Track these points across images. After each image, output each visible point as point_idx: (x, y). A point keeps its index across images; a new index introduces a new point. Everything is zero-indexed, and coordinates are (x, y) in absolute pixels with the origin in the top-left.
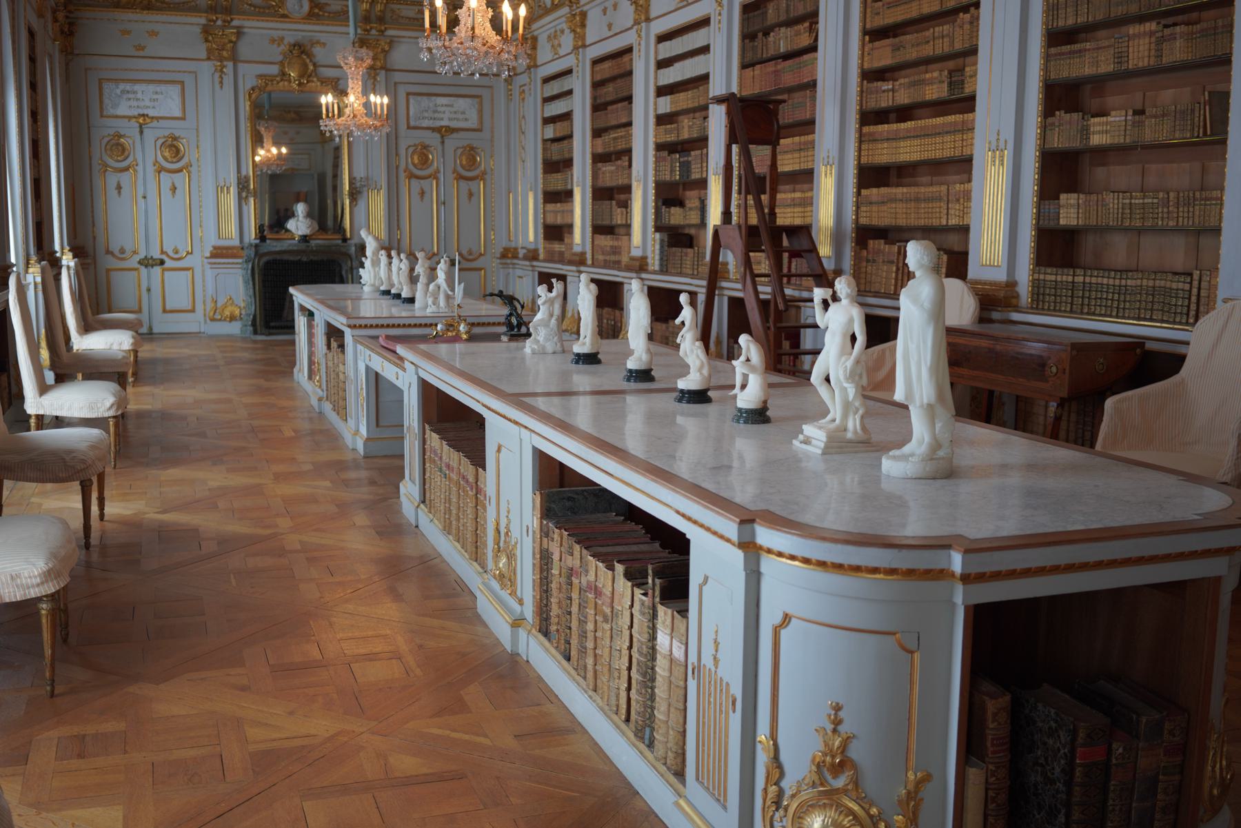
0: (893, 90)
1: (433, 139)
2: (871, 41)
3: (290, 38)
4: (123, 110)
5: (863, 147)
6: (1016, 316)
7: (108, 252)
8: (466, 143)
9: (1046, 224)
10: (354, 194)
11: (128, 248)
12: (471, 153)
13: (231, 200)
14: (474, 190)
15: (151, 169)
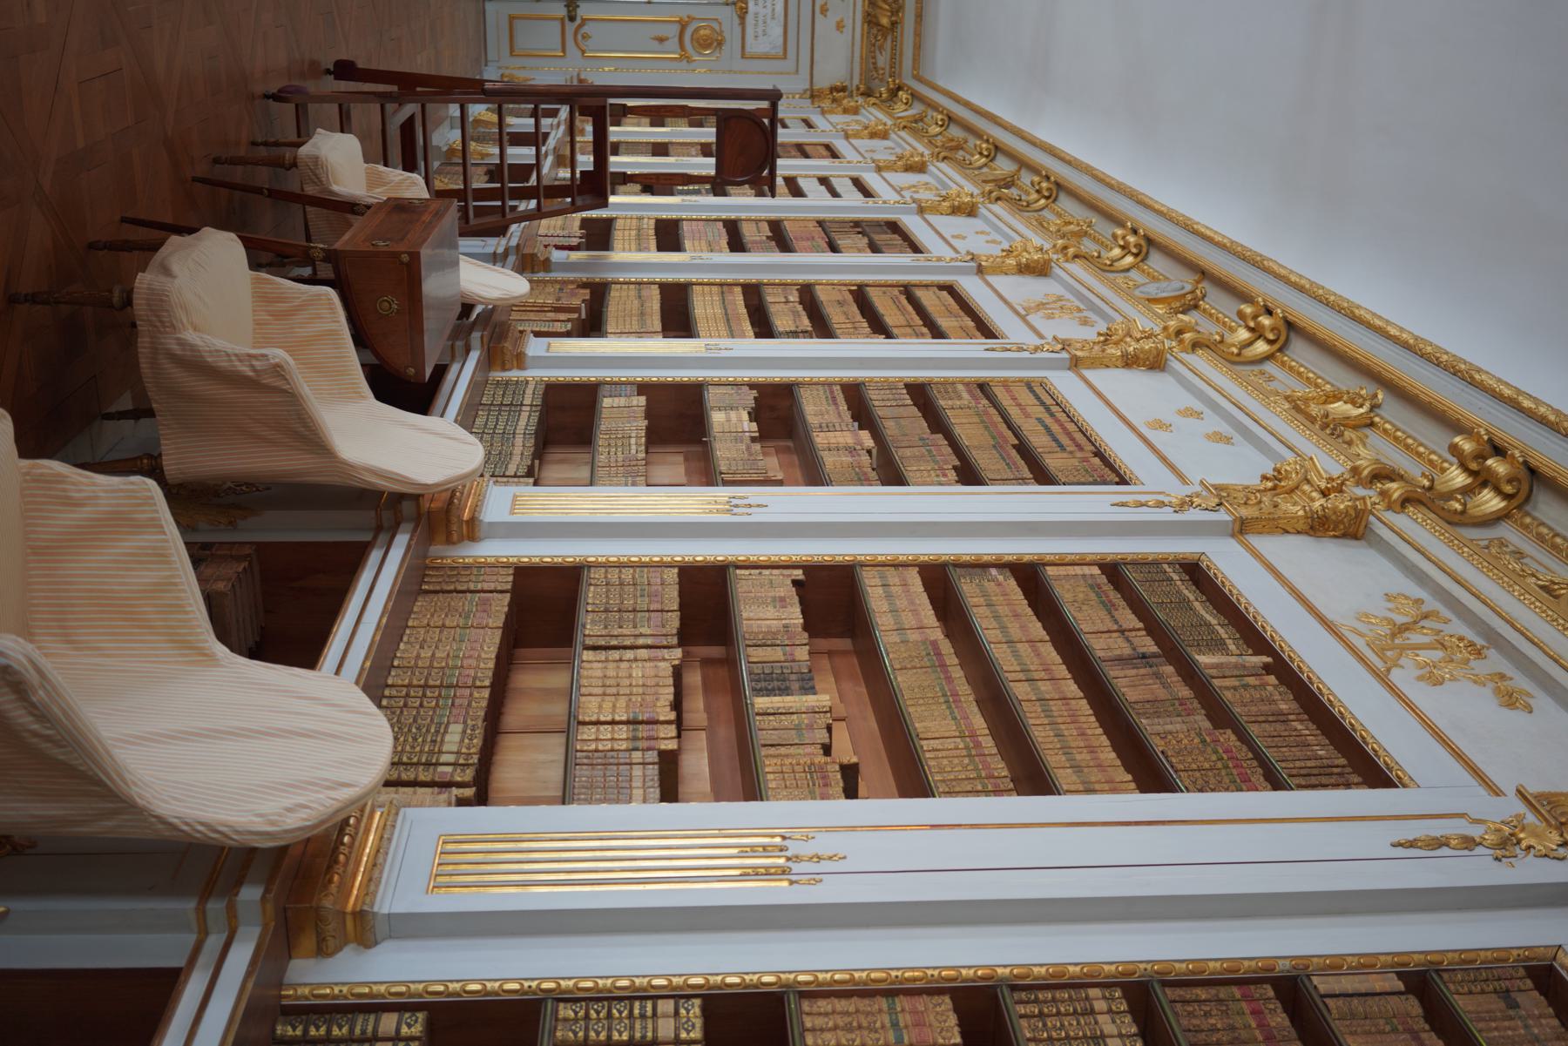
0: (787, 302)
2: (851, 292)
5: (715, 289)
6: (474, 356)
8: (727, 35)
9: (605, 390)
12: (713, 42)
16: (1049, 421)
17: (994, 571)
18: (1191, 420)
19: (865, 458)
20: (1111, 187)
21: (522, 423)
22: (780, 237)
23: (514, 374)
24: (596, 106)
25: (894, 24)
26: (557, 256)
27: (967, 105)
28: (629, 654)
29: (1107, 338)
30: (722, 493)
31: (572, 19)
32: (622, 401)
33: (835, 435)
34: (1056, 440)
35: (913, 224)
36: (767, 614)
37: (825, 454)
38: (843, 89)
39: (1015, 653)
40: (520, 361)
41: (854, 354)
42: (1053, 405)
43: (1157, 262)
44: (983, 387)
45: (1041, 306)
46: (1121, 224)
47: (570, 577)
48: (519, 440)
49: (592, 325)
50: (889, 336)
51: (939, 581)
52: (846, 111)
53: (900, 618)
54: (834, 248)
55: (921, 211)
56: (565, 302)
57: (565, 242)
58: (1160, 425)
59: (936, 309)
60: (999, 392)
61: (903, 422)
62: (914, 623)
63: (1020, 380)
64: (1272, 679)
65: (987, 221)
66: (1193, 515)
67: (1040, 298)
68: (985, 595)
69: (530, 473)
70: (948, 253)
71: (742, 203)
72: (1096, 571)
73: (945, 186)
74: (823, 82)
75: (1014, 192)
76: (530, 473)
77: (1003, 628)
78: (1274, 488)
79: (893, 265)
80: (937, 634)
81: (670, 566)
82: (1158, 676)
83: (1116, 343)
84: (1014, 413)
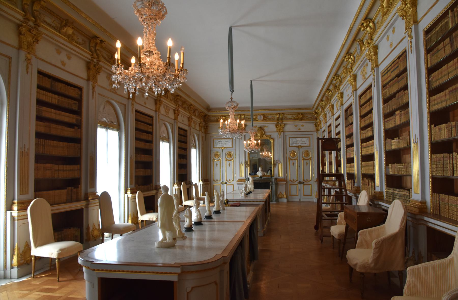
1: (296, 149)
3: (259, 126)
4: (218, 146)
5: (363, 150)
6: (380, 203)
7: (214, 180)
10: (275, 165)
11: (218, 179)
12: (307, 152)
13: (243, 167)
14: (308, 163)
15: (224, 160)
16: (391, 70)
17: (430, 79)
18: (390, 37)
19: (402, 112)
20: (335, 63)
21: (396, 192)
22: (350, 136)
23: (385, 194)
24: (321, 177)
25: (302, 114)
26: (356, 185)
27: (318, 97)
28: (455, 165)
29: (371, 60)
30: (413, 145)
31: (303, 183)
32: (390, 170)
33: (397, 120)
34: (396, 68)
35: (345, 106)
36: (443, 132)
37: (402, 122)
38: (316, 124)
39: (451, 72)
40: (381, 193)
41: (377, 117)
42: (388, 70)
43: (352, 51)
44: (384, 87)
45: (363, 75)
46: (344, 60)
47: (435, 180)
48: (401, 193)
49: (372, 177)
50: (372, 109)
51: (432, 92)
52: (321, 123)
53: (443, 100)
54: (352, 123)
55: (342, 105)
56: (367, 183)
57: (353, 183)
58: (391, 45)
59: (365, 99)
60: (385, 83)
61: (393, 104)
62: (444, 97)
63: (382, 78)
64: (455, 9)
65: (344, 90)
66: (413, 34)
67: (362, 76)
68: (436, 81)
69: (409, 190)
70: (352, 98)
71: (342, 145)
72: (429, 55)
73: (337, 100)
74: (314, 129)
75: (337, 85)
76: (409, 190)
77: (445, 75)
78: (405, 16)
79: (355, 111)
80: (447, 91)
81: (431, 156)
82: (455, 37)
83: (372, 57)
84: (389, 79)
